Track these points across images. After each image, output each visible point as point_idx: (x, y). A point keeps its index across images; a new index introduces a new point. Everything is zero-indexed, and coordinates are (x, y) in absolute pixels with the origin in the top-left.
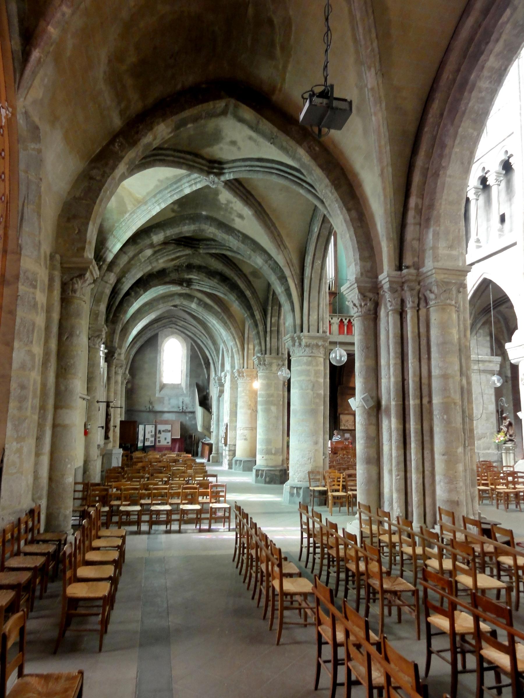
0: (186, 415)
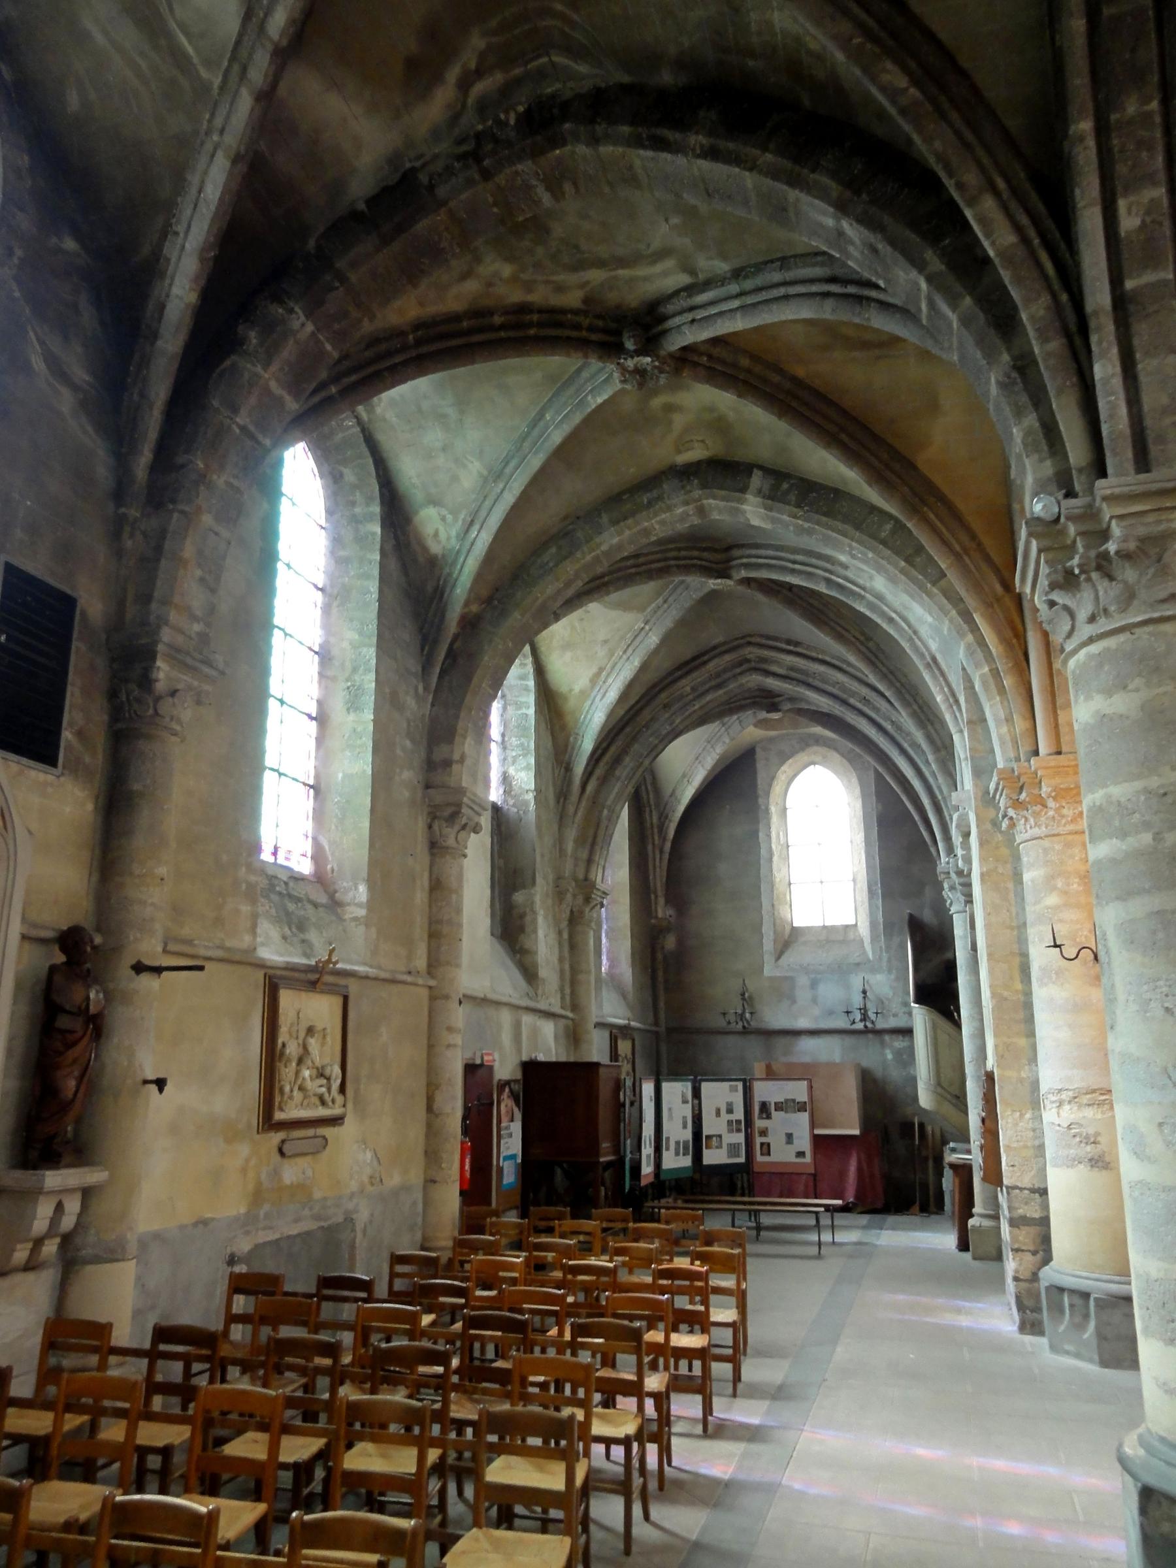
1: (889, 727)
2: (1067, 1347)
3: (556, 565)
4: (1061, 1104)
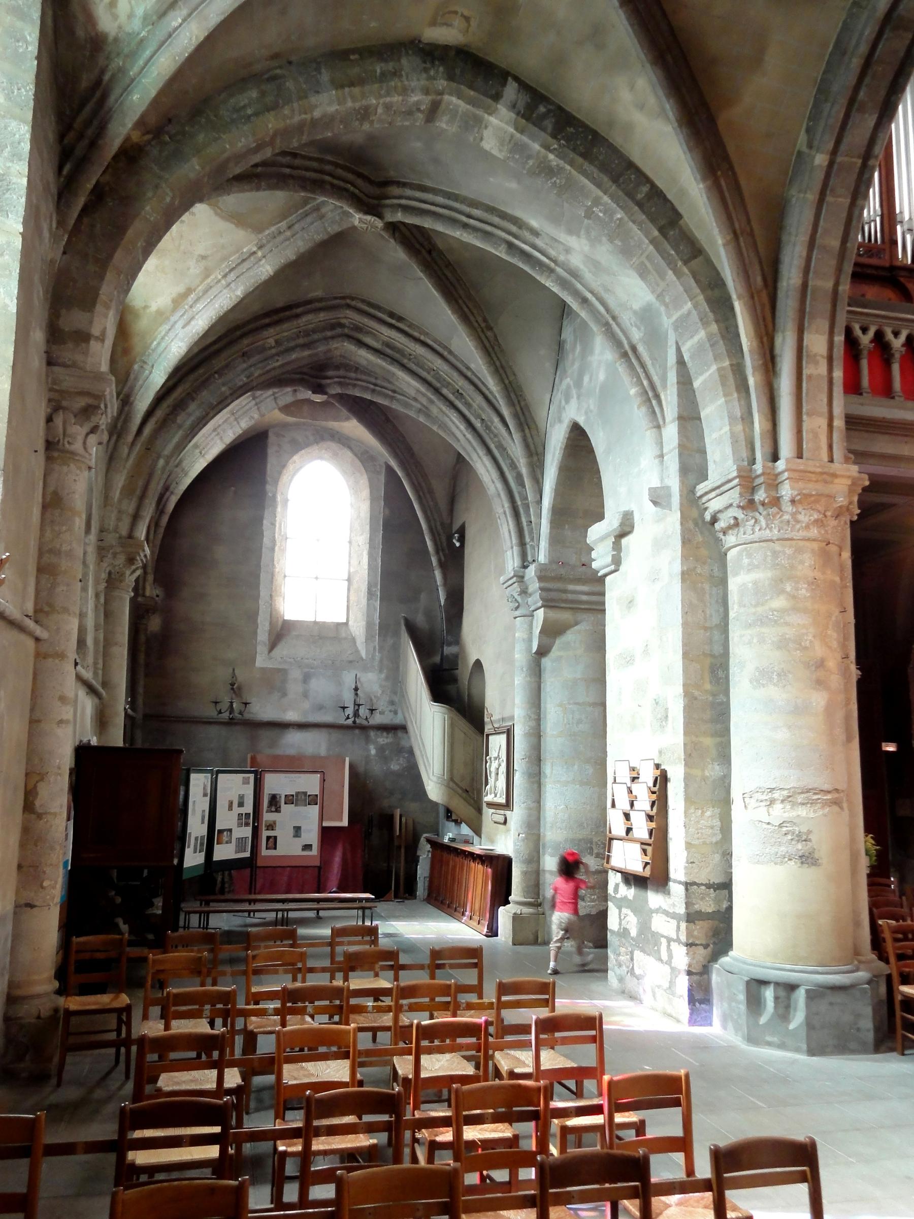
0: (368, 740)
1: (478, 424)
2: (769, 1038)
3: (256, 114)
4: (772, 802)
